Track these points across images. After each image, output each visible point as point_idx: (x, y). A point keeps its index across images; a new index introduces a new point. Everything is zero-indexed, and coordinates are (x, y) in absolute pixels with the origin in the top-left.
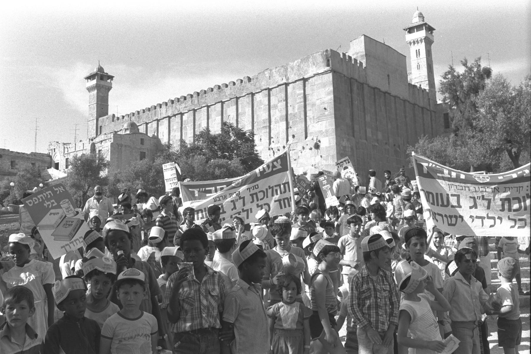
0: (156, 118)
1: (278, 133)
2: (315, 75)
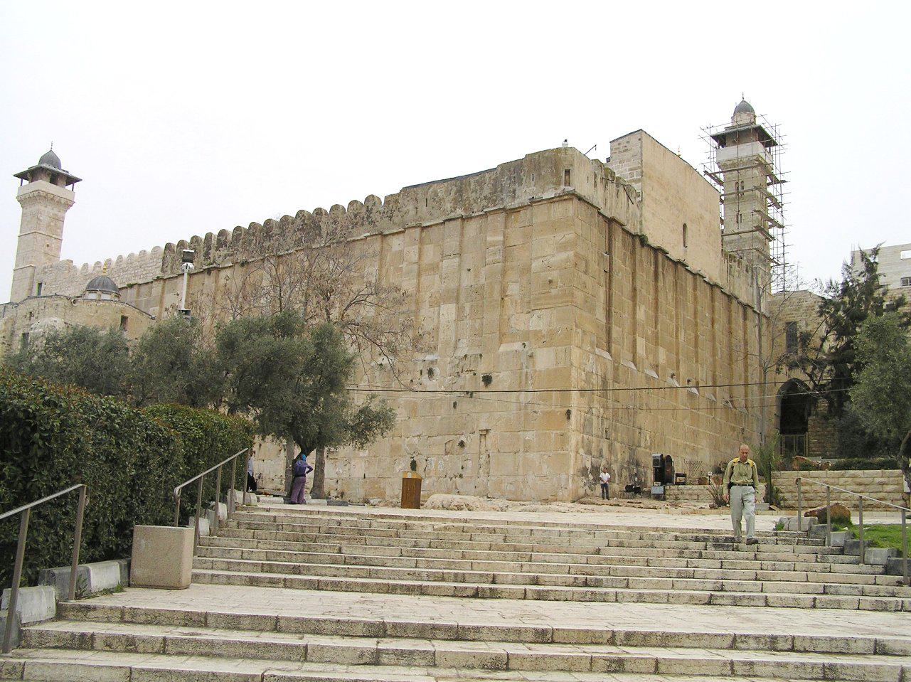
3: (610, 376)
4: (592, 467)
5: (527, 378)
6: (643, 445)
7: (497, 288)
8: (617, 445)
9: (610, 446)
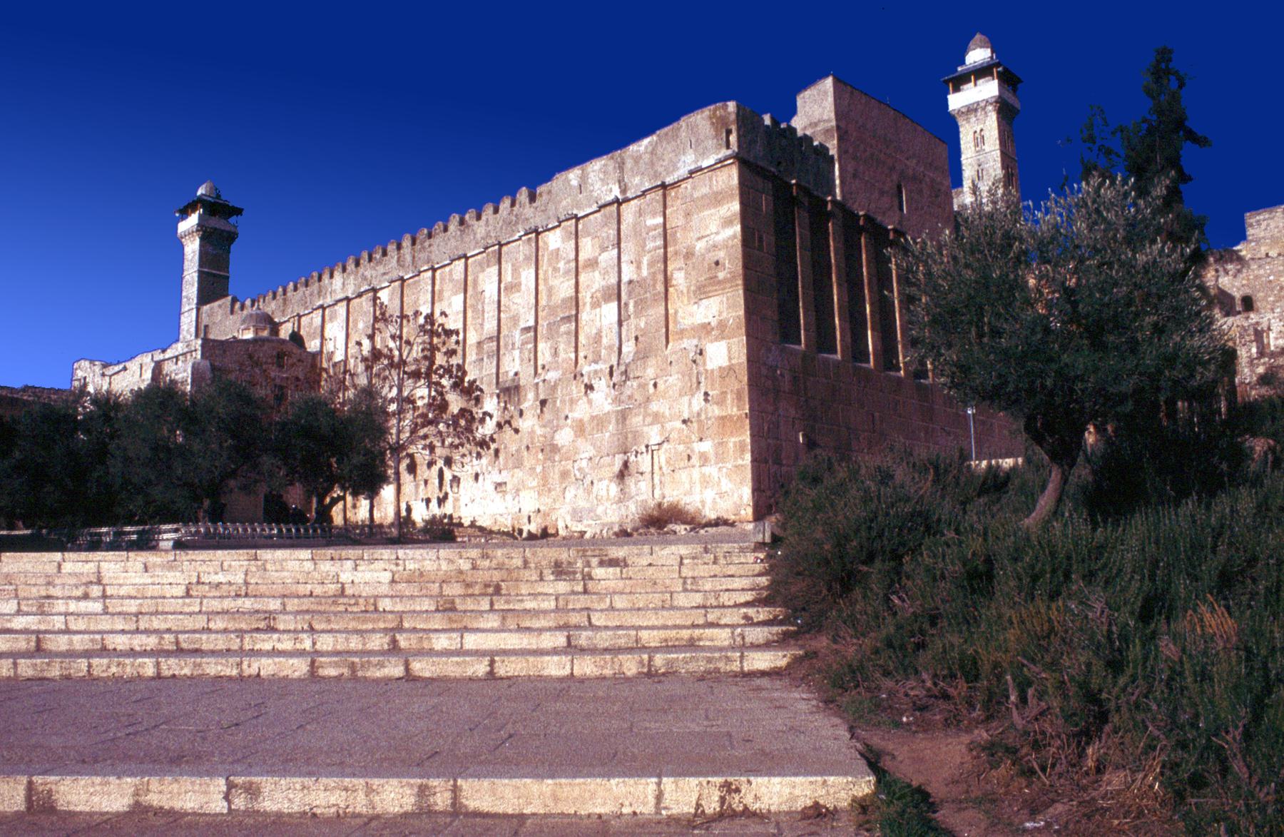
0: (321, 302)
2: (692, 172)
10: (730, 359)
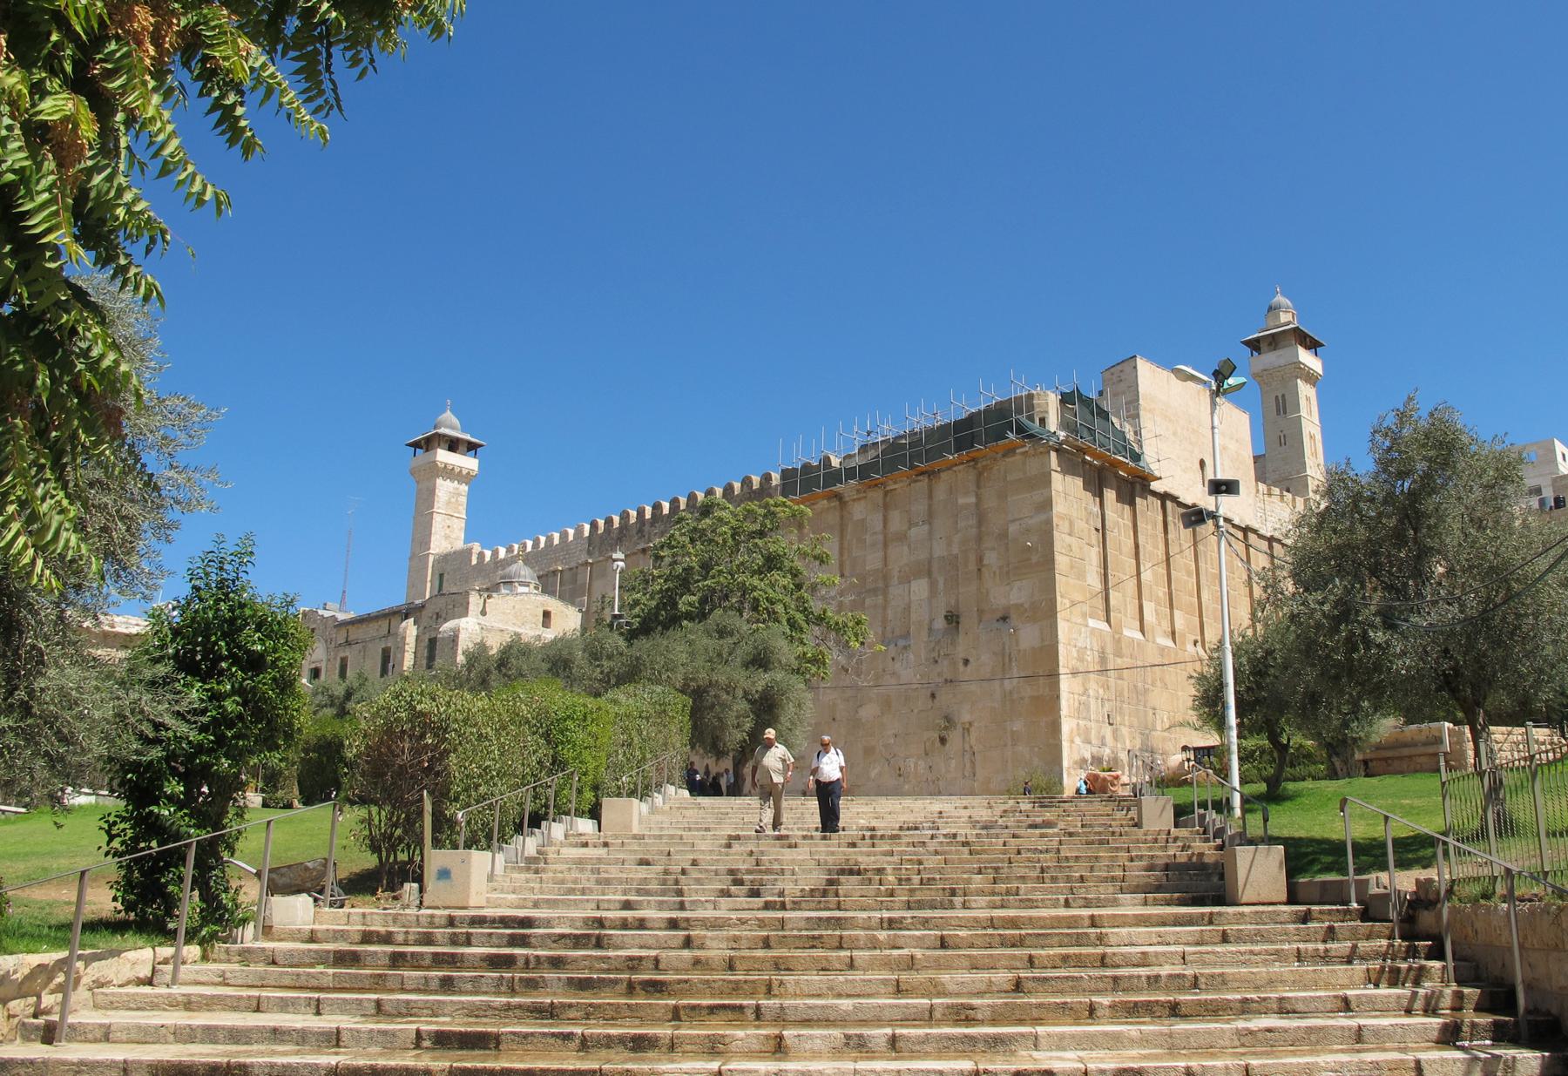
1: (908, 608)
3: (1109, 650)
4: (1093, 757)
5: (1010, 660)
6: (1159, 728)
7: (972, 557)
8: (1125, 731)
9: (1115, 732)
10: (1042, 640)
